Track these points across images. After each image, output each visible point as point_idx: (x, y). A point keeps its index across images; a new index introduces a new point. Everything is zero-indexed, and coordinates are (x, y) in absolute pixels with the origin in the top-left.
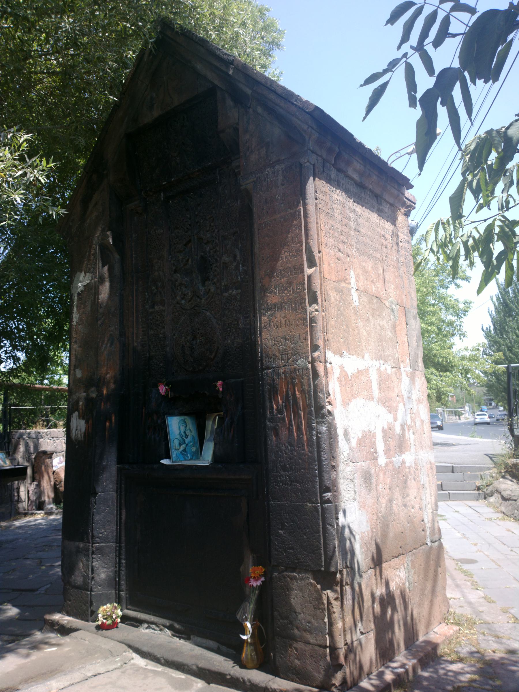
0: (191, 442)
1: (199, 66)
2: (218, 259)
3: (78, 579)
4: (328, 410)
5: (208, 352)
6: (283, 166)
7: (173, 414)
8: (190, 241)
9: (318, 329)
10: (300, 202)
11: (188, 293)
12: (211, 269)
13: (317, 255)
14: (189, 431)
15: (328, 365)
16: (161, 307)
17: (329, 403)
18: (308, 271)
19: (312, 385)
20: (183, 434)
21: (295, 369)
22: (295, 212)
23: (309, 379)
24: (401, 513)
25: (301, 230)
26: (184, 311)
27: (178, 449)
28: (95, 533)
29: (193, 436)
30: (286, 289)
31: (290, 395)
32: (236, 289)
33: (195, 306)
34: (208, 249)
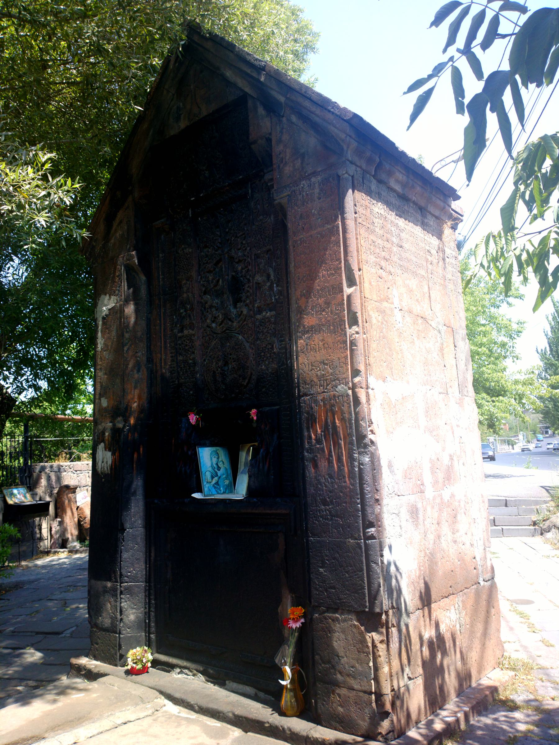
0: (224, 474)
1: (229, 74)
2: (251, 279)
3: (105, 621)
4: (371, 440)
5: (241, 378)
6: (319, 178)
7: (204, 445)
8: (220, 260)
9: (359, 352)
10: (338, 217)
11: (219, 316)
12: (244, 289)
13: (357, 274)
14: (221, 463)
15: (370, 391)
16: (191, 331)
17: (372, 431)
18: (347, 291)
19: (353, 413)
20: (215, 466)
21: (334, 396)
22: (333, 228)
23: (350, 407)
24: (451, 550)
25: (340, 247)
26: (215, 335)
27: (211, 482)
28: (123, 571)
29: (225, 468)
30: (324, 310)
31: (330, 423)
32: (270, 311)
33: (226, 329)
34: (240, 268)
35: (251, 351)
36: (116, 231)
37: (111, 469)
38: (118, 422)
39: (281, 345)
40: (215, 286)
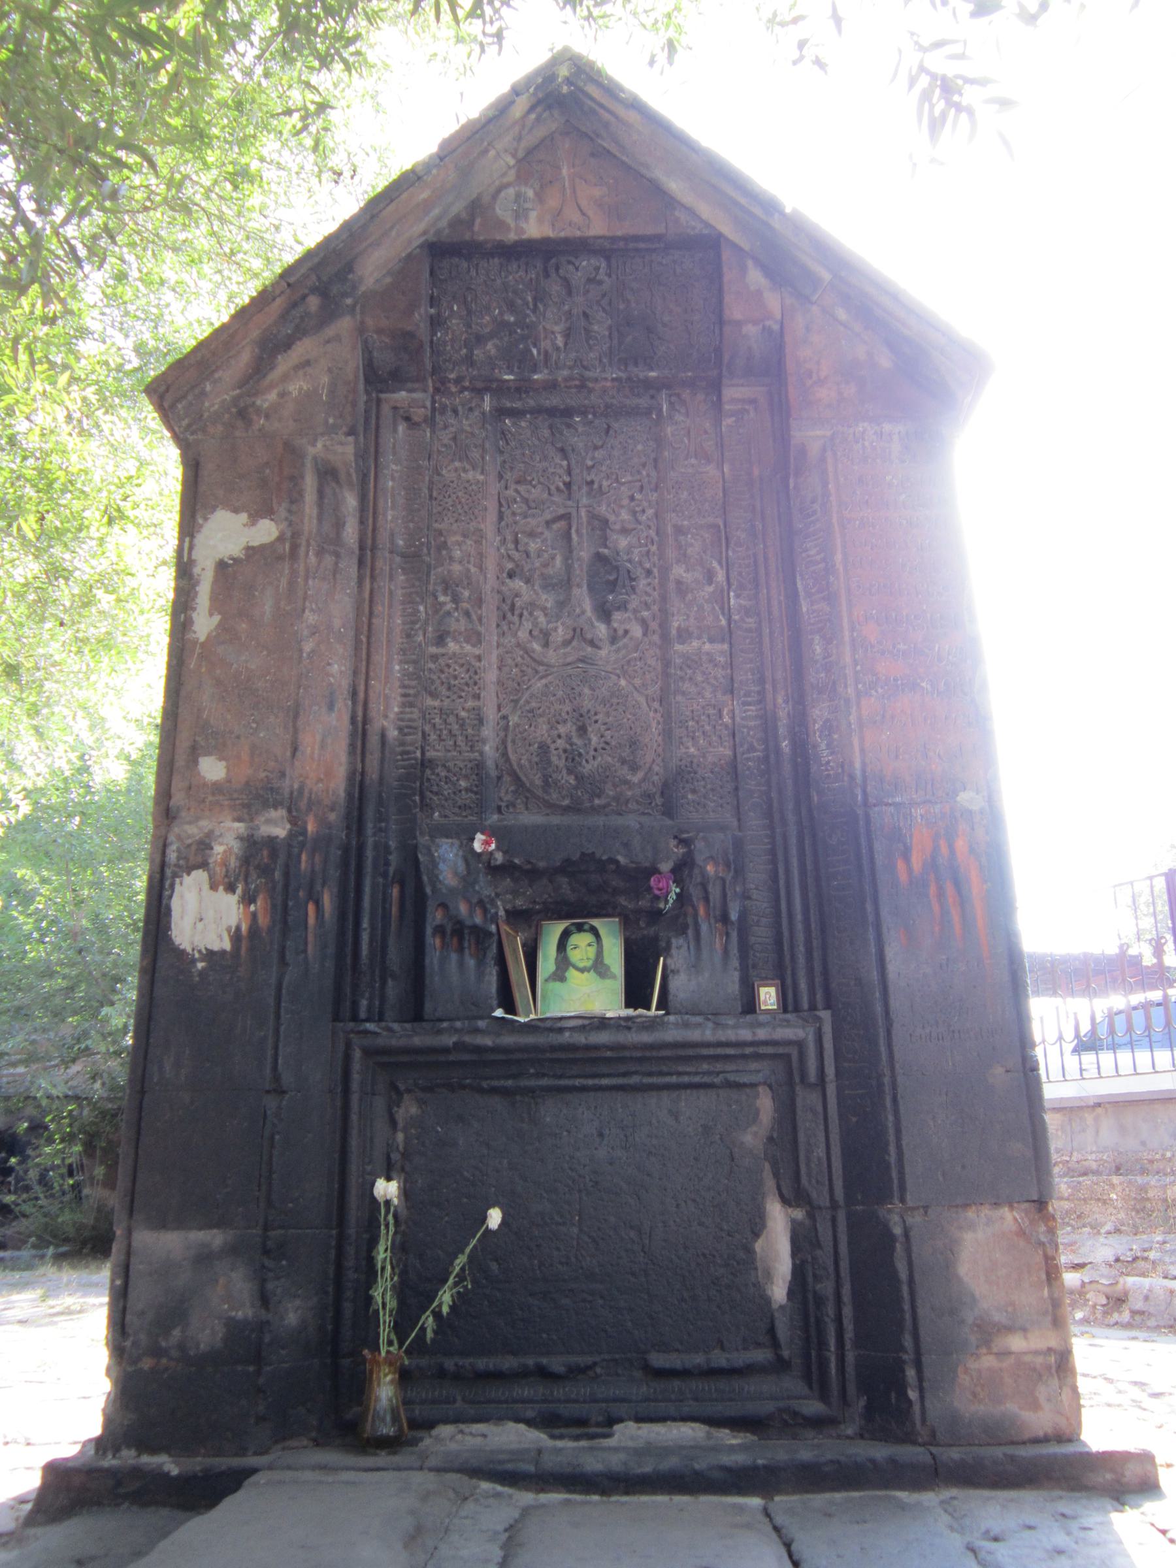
2: (655, 571)
5: (626, 767)
12: (633, 588)
16: (468, 648)
26: (541, 668)
35: (652, 714)
36: (285, 378)
37: (236, 937)
38: (269, 821)
40: (546, 565)
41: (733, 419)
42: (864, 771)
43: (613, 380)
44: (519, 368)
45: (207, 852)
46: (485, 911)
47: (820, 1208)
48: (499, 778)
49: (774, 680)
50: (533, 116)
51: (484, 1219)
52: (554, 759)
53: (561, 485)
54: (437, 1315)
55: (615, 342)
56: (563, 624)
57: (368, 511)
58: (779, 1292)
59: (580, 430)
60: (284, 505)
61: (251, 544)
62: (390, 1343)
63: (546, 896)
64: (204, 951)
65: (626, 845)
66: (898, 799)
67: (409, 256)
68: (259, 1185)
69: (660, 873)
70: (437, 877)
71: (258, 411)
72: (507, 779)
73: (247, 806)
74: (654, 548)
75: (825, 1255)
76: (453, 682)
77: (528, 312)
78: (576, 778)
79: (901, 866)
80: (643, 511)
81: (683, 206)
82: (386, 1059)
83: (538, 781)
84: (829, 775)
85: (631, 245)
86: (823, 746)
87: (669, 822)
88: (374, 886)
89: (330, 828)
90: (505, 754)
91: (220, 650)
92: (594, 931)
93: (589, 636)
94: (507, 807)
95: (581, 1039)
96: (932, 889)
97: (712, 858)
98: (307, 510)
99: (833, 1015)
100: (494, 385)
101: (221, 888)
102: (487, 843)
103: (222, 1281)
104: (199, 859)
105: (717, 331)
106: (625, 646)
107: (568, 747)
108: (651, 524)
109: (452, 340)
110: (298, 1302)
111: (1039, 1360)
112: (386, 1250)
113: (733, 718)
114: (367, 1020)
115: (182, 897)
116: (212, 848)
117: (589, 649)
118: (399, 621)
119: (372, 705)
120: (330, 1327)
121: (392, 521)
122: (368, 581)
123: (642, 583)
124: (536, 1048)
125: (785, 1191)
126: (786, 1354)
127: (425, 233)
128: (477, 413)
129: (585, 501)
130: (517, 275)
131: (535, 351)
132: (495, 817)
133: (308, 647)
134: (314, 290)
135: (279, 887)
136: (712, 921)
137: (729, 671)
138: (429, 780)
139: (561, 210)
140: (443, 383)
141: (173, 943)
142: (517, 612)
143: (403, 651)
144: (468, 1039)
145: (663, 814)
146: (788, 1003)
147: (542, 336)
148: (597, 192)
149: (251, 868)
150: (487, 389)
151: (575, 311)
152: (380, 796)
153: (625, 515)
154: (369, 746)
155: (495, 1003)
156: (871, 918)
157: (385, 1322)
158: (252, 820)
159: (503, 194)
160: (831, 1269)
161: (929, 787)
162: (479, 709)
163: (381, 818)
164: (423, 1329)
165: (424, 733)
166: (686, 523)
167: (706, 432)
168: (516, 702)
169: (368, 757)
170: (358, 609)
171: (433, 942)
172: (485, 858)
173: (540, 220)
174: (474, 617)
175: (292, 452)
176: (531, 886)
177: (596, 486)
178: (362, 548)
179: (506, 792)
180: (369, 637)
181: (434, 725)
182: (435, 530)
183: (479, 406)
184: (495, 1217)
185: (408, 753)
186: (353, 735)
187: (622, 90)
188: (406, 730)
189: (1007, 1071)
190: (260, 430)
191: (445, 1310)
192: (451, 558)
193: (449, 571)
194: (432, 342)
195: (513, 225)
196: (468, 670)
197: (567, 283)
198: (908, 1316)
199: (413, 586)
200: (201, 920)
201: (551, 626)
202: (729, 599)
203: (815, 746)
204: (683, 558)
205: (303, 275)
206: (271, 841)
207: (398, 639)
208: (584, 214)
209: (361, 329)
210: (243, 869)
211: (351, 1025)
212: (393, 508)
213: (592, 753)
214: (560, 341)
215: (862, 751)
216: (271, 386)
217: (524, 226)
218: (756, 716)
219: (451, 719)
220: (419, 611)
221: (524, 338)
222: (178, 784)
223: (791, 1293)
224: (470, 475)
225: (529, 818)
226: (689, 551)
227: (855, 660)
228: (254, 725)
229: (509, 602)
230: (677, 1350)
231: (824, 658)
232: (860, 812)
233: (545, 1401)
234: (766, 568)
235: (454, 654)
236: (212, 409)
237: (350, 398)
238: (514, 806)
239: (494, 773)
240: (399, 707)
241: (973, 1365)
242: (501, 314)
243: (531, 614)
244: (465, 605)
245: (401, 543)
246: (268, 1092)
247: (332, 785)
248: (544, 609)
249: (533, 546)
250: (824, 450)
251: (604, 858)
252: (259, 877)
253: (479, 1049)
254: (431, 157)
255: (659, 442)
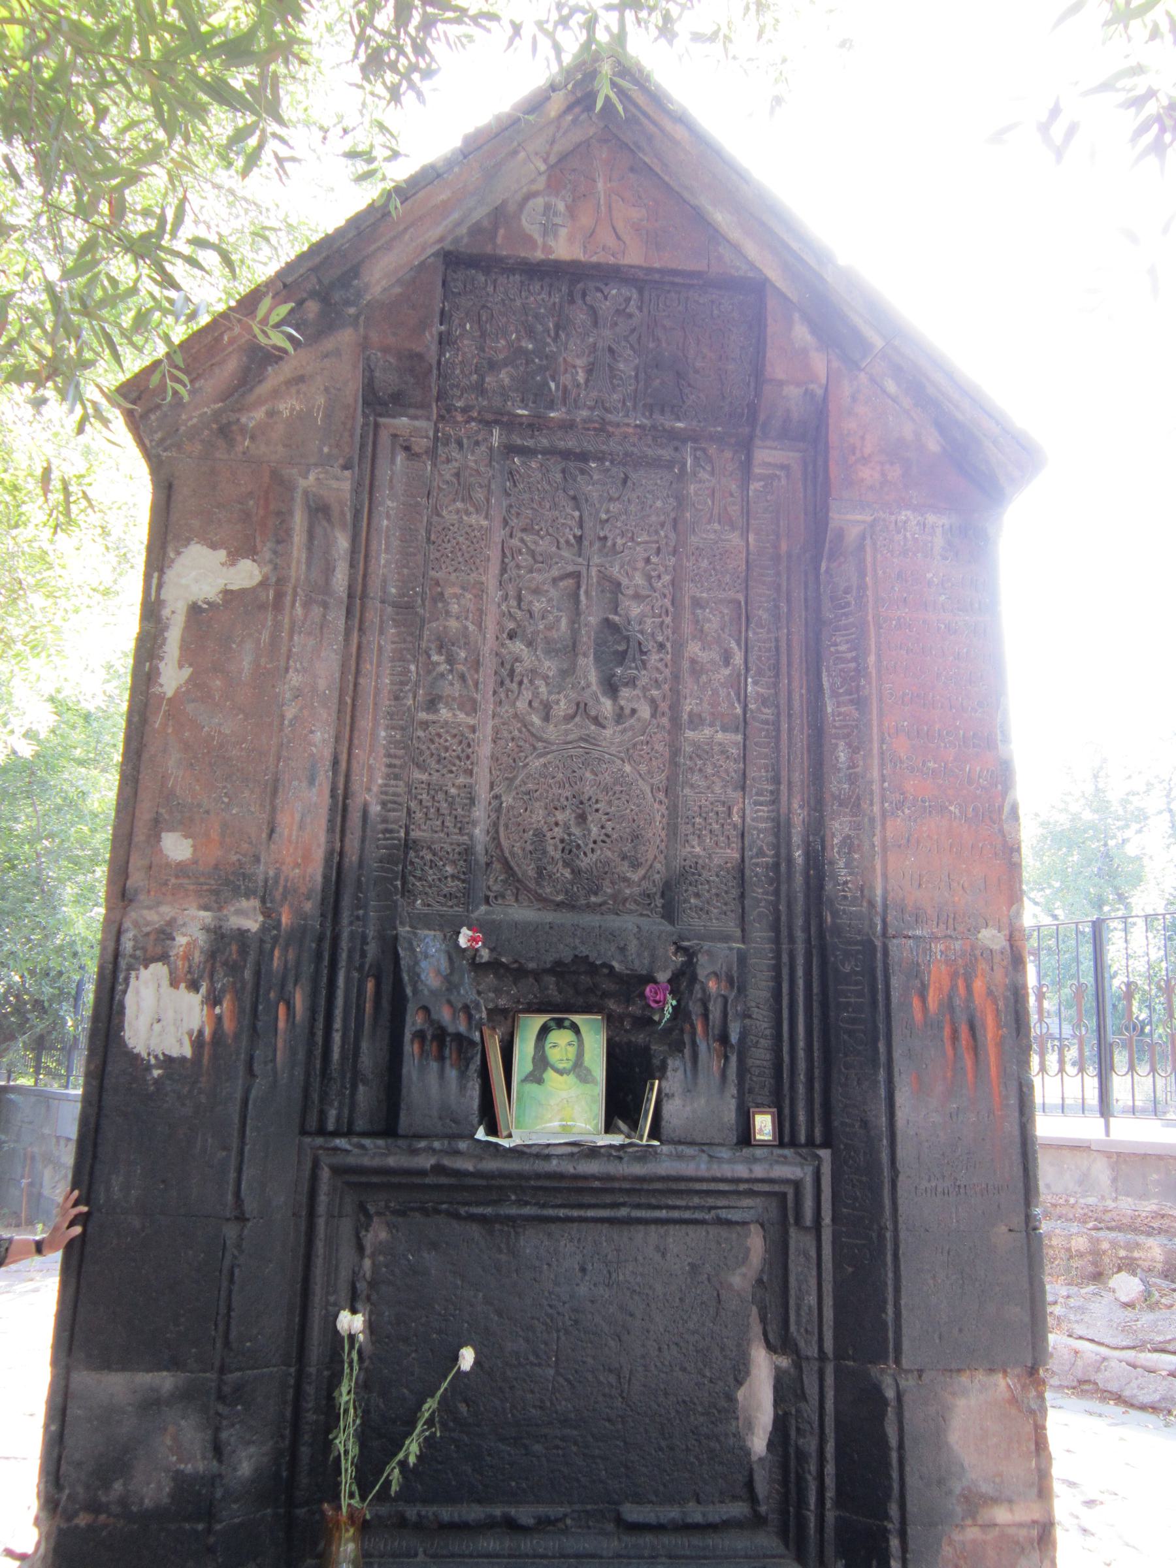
2: (668, 645)
5: (626, 863)
12: (644, 663)
16: (461, 716)
35: (656, 806)
36: (276, 394)
37: (198, 1042)
38: (239, 912)
39: (756, 811)
40: (549, 628)
41: (762, 483)
42: (885, 899)
43: (636, 426)
44: (534, 402)
45: (168, 942)
46: (470, 1017)
47: (807, 1358)
48: (488, 865)
49: (790, 783)
50: (569, 118)
51: (456, 1358)
52: (550, 849)
53: (571, 537)
54: (403, 1464)
55: (642, 383)
56: (566, 697)
57: (360, 554)
58: (759, 1443)
59: (596, 477)
60: (269, 545)
61: (230, 587)
62: (352, 1496)
63: (531, 996)
64: (161, 1057)
65: (622, 950)
66: (918, 933)
67: (423, 263)
68: (216, 1325)
69: (655, 982)
70: (419, 976)
71: (243, 430)
72: (497, 866)
73: (217, 893)
74: (668, 620)
75: (810, 1410)
76: (443, 755)
77: (549, 340)
78: (573, 872)
79: (916, 1003)
80: (659, 577)
81: (728, 241)
82: (354, 1179)
83: (531, 873)
84: (845, 897)
85: (667, 279)
86: (841, 864)
87: (669, 928)
88: (348, 979)
89: (305, 919)
90: (496, 839)
91: (190, 708)
92: (575, 1028)
93: (593, 713)
94: (496, 897)
95: (568, 1168)
96: (947, 1032)
97: (715, 974)
98: (295, 554)
99: (833, 1154)
100: (505, 419)
101: (183, 985)
102: (473, 939)
103: (171, 1429)
104: (159, 950)
105: (752, 385)
106: (632, 728)
107: (566, 837)
108: (667, 592)
109: (462, 362)
110: (252, 1449)
111: (1023, 1532)
112: (349, 1392)
113: (743, 818)
114: (336, 1134)
115: (137, 992)
116: (173, 939)
117: (593, 727)
118: (387, 681)
119: (355, 778)
120: (285, 1474)
121: (385, 566)
122: (355, 634)
123: (654, 658)
124: (520, 1176)
125: (772, 1340)
126: (763, 1509)
127: (441, 239)
128: (483, 448)
129: (596, 560)
130: (539, 297)
131: (553, 385)
132: (483, 908)
133: (290, 712)
134: (313, 294)
135: (249, 987)
136: (711, 1042)
137: (741, 765)
138: (412, 863)
139: (593, 232)
140: (449, 411)
141: (125, 1046)
142: (517, 679)
143: (391, 715)
144: (447, 1162)
145: (663, 917)
146: (785, 1137)
147: (562, 368)
148: (636, 214)
149: (218, 964)
150: (496, 422)
151: (600, 345)
152: (359, 881)
153: (639, 579)
154: (349, 824)
155: (475, 1119)
156: (883, 1058)
157: (346, 1470)
158: (220, 909)
159: (531, 204)
160: (816, 1425)
161: (951, 921)
162: (471, 787)
163: (359, 904)
164: (388, 1483)
165: (409, 809)
166: (704, 595)
167: (732, 495)
168: (511, 780)
169: (349, 836)
170: (344, 666)
171: (411, 1049)
172: (470, 953)
173: (571, 239)
174: (470, 682)
175: (280, 484)
176: (515, 984)
177: (609, 543)
178: (350, 596)
179: (494, 881)
180: (354, 700)
181: (421, 801)
182: (432, 579)
183: (485, 440)
184: (467, 1358)
185: (391, 831)
186: (332, 810)
187: (671, 101)
188: (390, 805)
189: (1010, 1230)
190: (244, 453)
191: (412, 1460)
192: (448, 613)
193: (445, 627)
194: (439, 362)
195: (540, 241)
196: (460, 742)
197: (593, 312)
198: (896, 1486)
199: (405, 641)
200: (159, 1021)
201: (553, 697)
202: (746, 685)
203: (832, 863)
204: (700, 635)
205: (301, 276)
206: (242, 934)
207: (386, 702)
208: (618, 237)
209: (364, 345)
210: (209, 965)
211: (320, 1141)
212: (387, 550)
213: (591, 845)
214: (581, 377)
215: (885, 876)
216: (259, 402)
217: (552, 243)
218: (768, 818)
219: (440, 796)
220: (410, 671)
221: (542, 369)
222: (137, 862)
223: (770, 1445)
224: (473, 519)
225: (522, 913)
226: (707, 626)
227: (883, 775)
228: (226, 800)
229: (508, 667)
230: (651, 1502)
231: (849, 768)
232: (878, 943)
233: (510, 1556)
234: (789, 655)
235: (446, 722)
236: (190, 423)
237: (349, 426)
238: (503, 897)
239: (483, 859)
240: (383, 778)
241: (957, 1536)
242: (518, 339)
243: (531, 682)
244: (461, 668)
245: (393, 590)
246: (228, 1220)
247: (309, 870)
248: (546, 678)
249: (537, 606)
250: (863, 537)
251: (598, 963)
252: (225, 976)
253: (458, 1173)
254: (454, 153)
255: (681, 501)
